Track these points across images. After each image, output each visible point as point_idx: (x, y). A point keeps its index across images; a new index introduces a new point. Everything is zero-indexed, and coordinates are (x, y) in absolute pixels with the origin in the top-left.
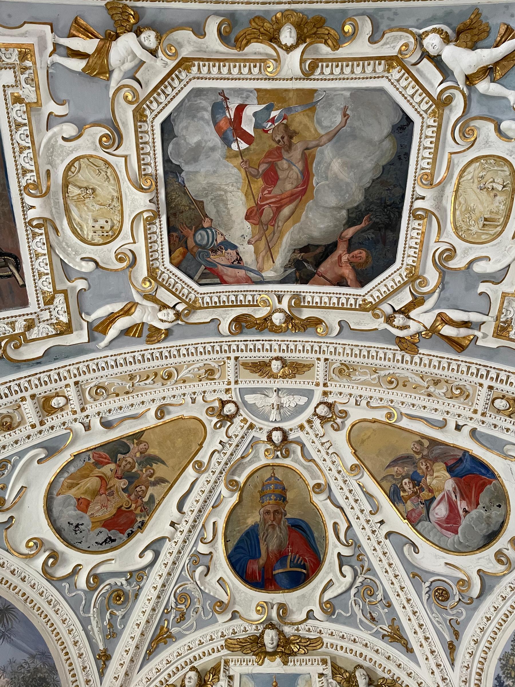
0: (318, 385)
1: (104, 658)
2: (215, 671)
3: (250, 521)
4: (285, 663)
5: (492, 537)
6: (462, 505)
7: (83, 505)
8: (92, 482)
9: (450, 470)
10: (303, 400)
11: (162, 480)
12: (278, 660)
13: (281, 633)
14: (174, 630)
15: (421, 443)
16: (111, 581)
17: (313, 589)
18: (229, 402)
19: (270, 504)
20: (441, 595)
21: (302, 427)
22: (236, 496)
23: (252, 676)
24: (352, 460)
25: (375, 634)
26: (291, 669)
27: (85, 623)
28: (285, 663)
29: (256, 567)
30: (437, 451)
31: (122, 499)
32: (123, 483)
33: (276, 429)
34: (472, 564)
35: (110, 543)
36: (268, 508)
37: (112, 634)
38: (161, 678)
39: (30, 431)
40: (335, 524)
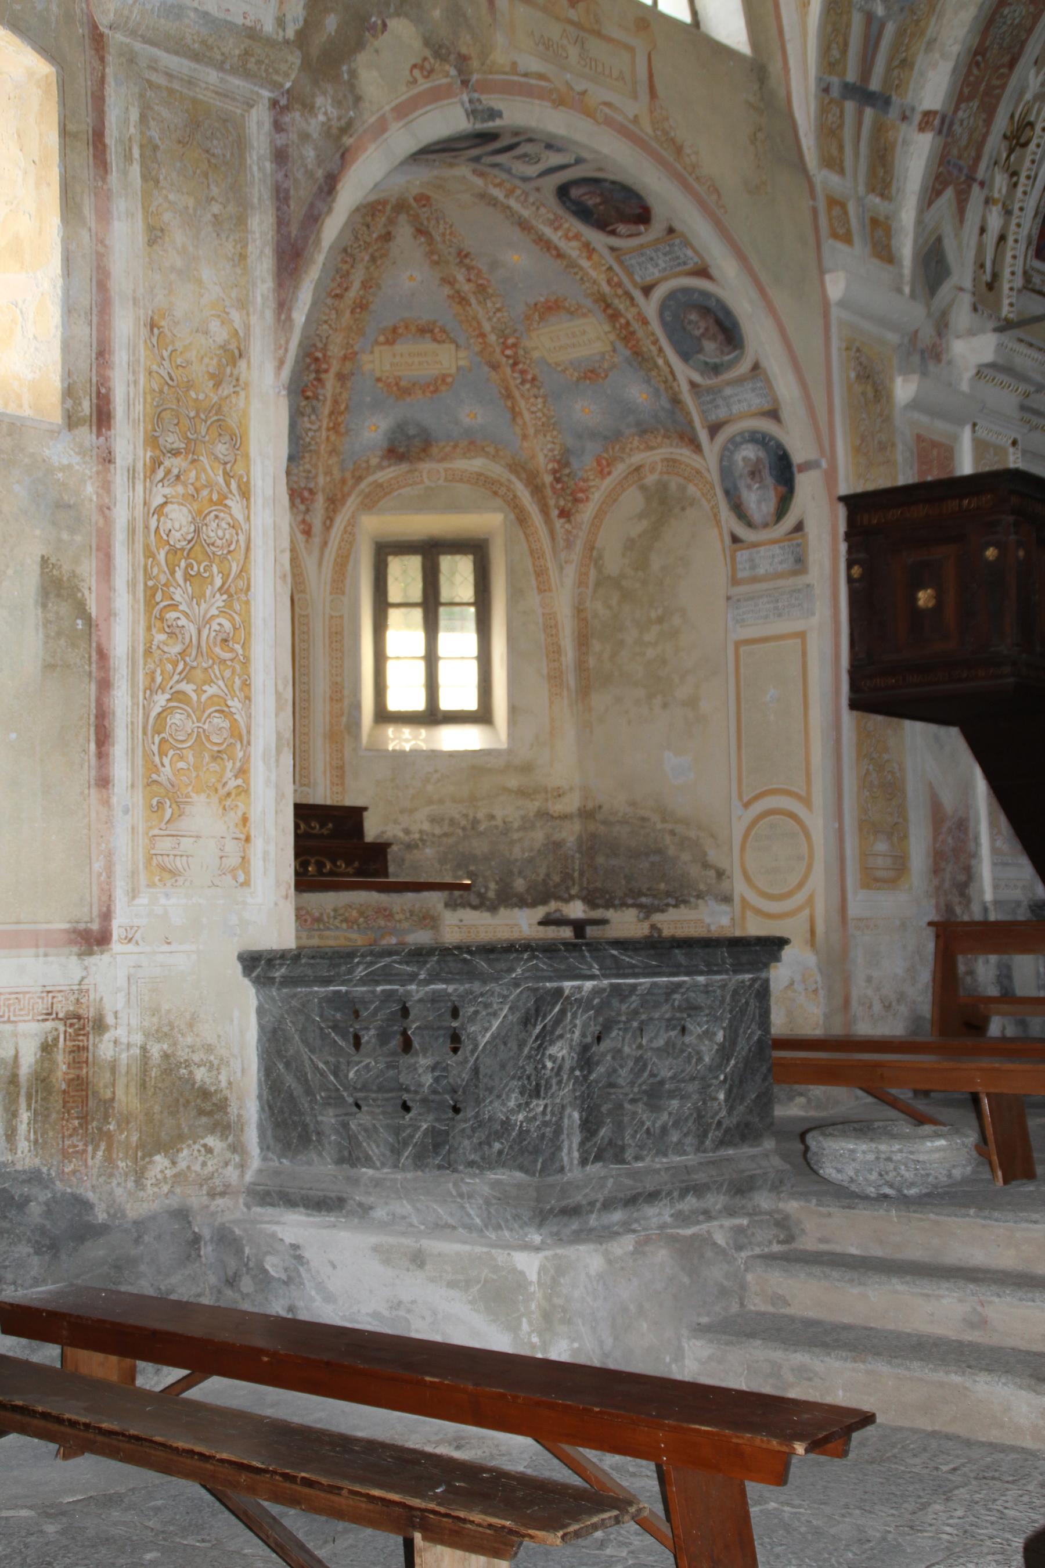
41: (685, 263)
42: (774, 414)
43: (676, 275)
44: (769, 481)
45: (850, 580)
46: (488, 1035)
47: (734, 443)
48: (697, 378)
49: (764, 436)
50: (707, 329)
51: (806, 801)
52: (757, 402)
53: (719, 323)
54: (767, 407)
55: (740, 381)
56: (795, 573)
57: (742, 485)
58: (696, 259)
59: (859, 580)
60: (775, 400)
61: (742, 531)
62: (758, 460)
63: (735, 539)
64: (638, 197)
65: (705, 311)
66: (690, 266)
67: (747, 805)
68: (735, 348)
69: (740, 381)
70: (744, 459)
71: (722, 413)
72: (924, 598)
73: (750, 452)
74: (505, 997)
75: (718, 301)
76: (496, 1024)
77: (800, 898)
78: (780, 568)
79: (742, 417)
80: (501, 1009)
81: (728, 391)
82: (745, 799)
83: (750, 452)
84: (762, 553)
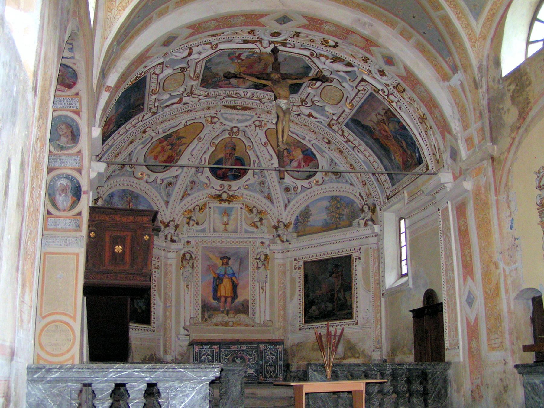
0: (256, 114)
1: (167, 203)
2: (205, 205)
3: (220, 157)
4: (229, 204)
5: (309, 177)
6: (303, 164)
7: (156, 158)
8: (159, 149)
9: (303, 152)
10: (248, 118)
11: (184, 144)
12: (227, 203)
13: (228, 194)
14: (189, 192)
15: (294, 141)
16: (168, 180)
17: (242, 181)
18: (215, 117)
19: (229, 150)
20: (287, 189)
21: (246, 127)
22: (214, 149)
23: (217, 207)
24: (264, 140)
25: (262, 196)
26: (231, 205)
27: (160, 193)
28: (229, 204)
29: (221, 172)
30: (300, 145)
31: (169, 153)
32: (170, 147)
33: (235, 127)
34: (300, 184)
35: (167, 168)
36: (228, 152)
37: (169, 195)
38: (186, 207)
39: (139, 141)
40: (254, 161)
41: (73, 107)
42: (80, 171)
43: (65, 110)
44: (70, 194)
45: (89, 237)
46: (183, 405)
47: (58, 177)
48: (52, 149)
49: (72, 177)
50: (66, 133)
51: (74, 318)
52: (74, 164)
53: (72, 132)
54: (77, 167)
55: (70, 155)
56: (76, 231)
57: (57, 194)
58: (79, 107)
59: (94, 237)
60: (82, 166)
61: (53, 210)
62: (67, 185)
63: (49, 213)
64: (77, 79)
65: (69, 126)
66: (75, 109)
67: (44, 317)
68: (74, 143)
69: (70, 155)
70: (60, 184)
71: (57, 165)
72: (119, 249)
73: (64, 182)
74: (193, 388)
75: (77, 124)
76: (187, 400)
77: (68, 356)
78: (68, 228)
79: (65, 168)
80: (191, 393)
81: (63, 157)
82: (43, 315)
83: (64, 182)
84: (61, 220)
